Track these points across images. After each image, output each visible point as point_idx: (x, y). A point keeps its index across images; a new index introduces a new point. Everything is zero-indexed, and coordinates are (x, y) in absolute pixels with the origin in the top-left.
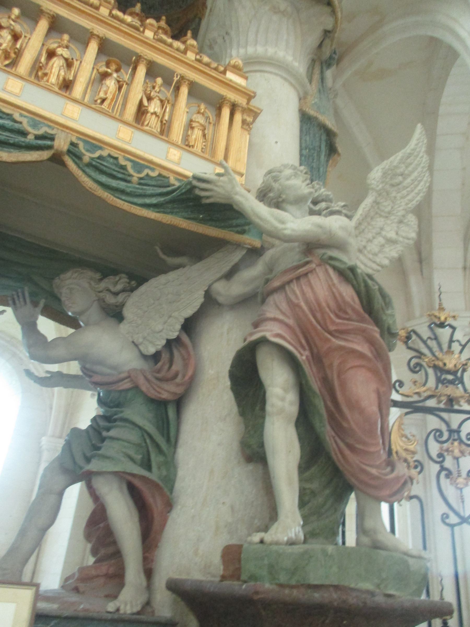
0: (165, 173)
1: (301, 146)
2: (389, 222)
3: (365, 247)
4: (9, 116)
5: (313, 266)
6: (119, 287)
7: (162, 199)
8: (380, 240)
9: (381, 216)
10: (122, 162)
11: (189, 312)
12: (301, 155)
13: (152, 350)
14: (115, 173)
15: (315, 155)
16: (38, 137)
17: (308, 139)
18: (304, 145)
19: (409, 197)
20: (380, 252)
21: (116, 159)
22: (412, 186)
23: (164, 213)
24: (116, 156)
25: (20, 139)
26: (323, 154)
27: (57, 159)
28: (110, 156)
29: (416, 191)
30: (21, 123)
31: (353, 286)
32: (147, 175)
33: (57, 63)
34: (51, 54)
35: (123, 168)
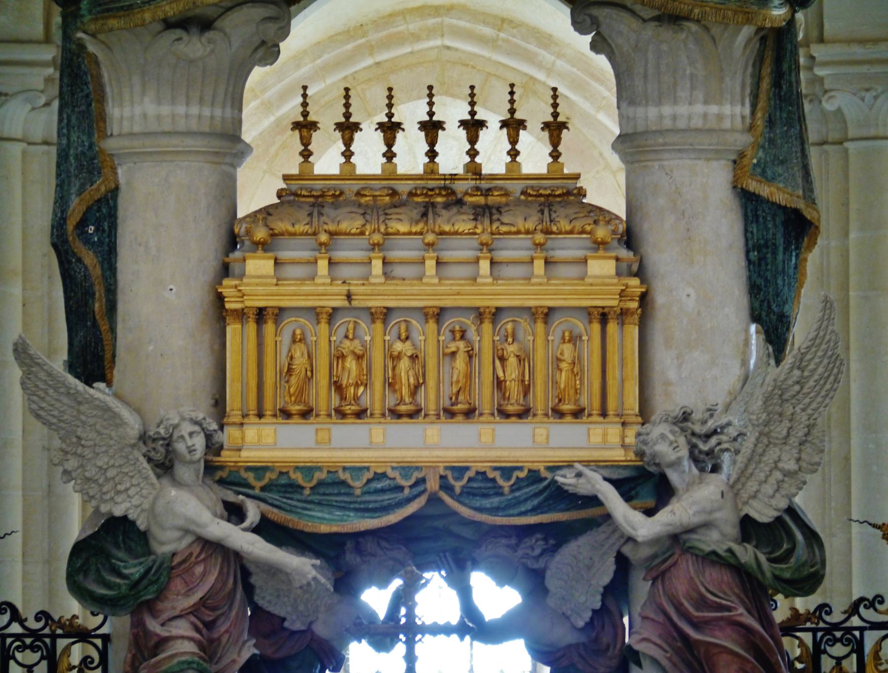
0: (534, 466)
1: (747, 244)
2: (787, 448)
3: (757, 491)
4: (384, 475)
5: (676, 556)
6: (537, 551)
7: (536, 502)
8: (778, 475)
9: (775, 445)
10: (491, 475)
11: (606, 579)
12: (749, 262)
13: (581, 624)
14: (486, 491)
15: (769, 255)
16: (411, 487)
17: (755, 231)
18: (750, 243)
19: (814, 405)
20: (777, 490)
21: (484, 473)
22: (817, 388)
23: (542, 513)
24: (483, 470)
25: (400, 496)
26: (781, 249)
27: (434, 499)
28: (478, 473)
29: (823, 393)
30: (394, 479)
31: (722, 565)
32: (518, 478)
33: (404, 364)
34: (396, 358)
35: (493, 480)
